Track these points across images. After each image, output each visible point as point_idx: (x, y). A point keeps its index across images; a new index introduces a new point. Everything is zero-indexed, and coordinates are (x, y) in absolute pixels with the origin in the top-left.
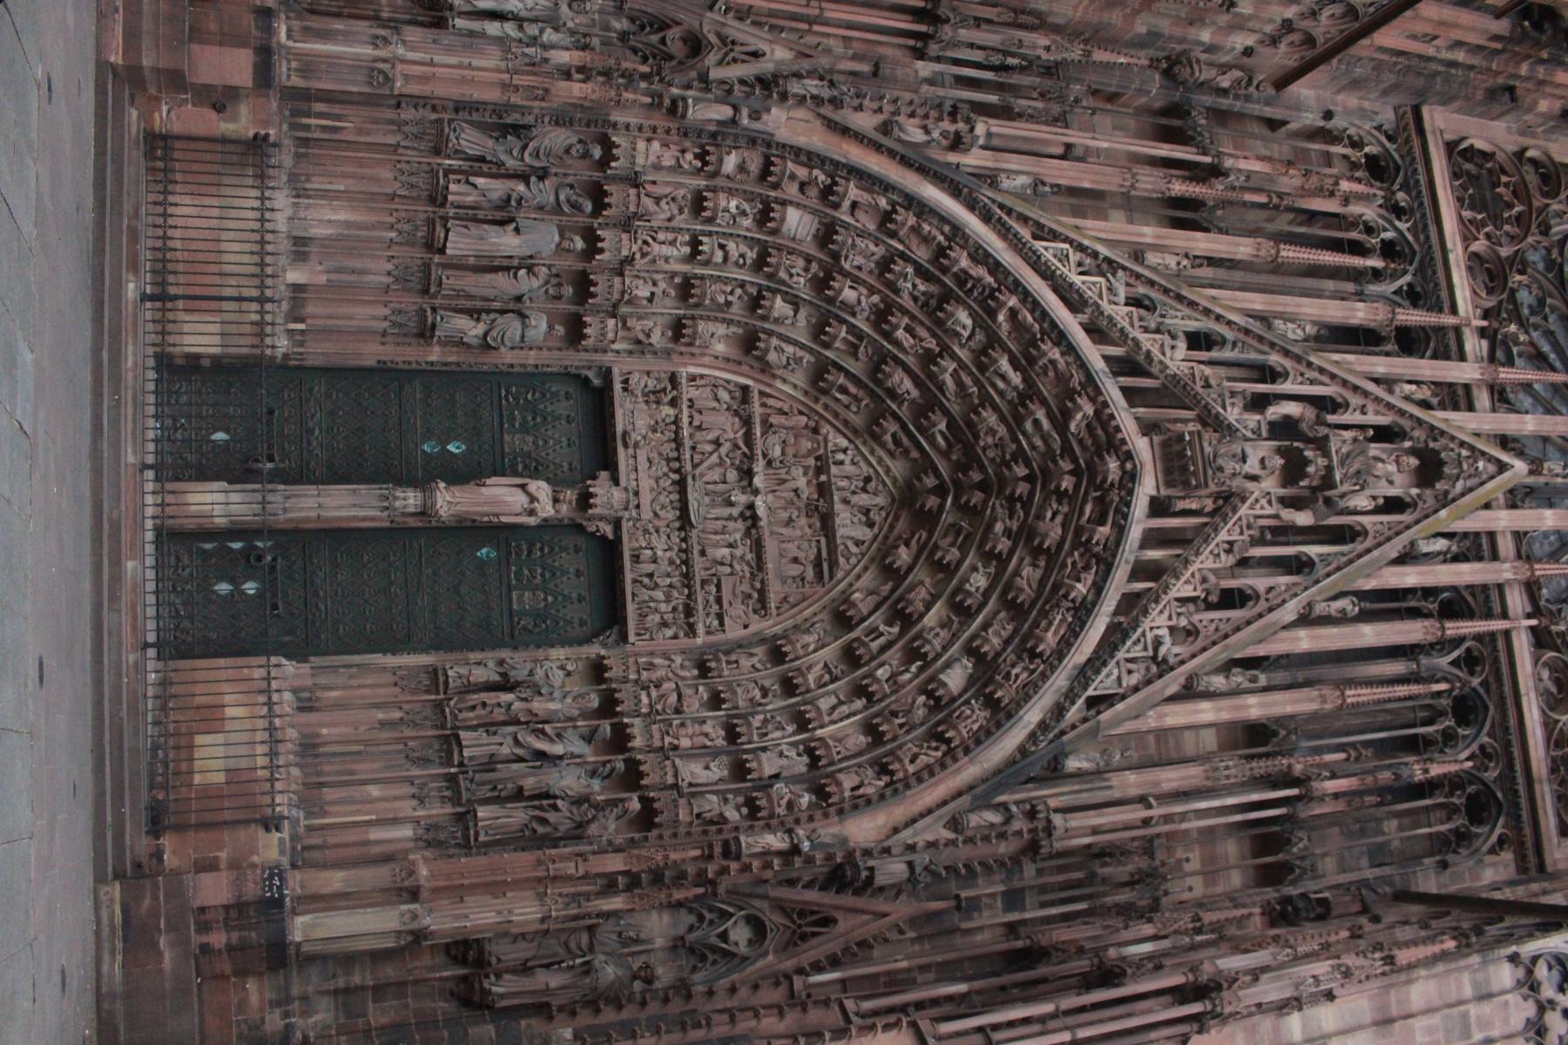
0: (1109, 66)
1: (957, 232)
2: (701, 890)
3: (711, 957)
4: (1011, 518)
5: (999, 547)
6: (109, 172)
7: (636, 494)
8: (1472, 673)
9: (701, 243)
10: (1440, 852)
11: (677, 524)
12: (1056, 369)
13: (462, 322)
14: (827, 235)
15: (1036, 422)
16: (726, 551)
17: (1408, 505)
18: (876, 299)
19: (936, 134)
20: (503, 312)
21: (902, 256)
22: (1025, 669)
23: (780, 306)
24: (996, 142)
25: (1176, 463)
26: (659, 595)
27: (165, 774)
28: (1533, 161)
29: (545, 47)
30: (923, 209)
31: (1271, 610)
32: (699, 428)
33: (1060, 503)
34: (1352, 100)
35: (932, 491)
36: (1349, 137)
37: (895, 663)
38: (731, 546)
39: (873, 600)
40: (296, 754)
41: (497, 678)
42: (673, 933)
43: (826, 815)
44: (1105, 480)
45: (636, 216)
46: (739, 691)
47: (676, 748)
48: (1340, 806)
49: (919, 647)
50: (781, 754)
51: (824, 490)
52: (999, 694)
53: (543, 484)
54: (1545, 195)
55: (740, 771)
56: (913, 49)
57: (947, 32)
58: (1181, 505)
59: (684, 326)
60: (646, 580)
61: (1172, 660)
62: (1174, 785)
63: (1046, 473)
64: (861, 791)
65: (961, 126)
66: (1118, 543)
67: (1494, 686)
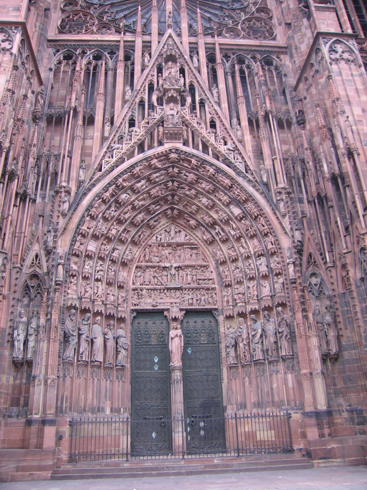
0: (38, 139)
1: (98, 196)
2: (305, 291)
3: (321, 289)
4: (184, 189)
5: (194, 193)
6: (90, 474)
7: (171, 303)
8: (230, 57)
9: (97, 278)
10: (281, 76)
11: (181, 291)
12: (142, 169)
13: (120, 357)
14: (95, 237)
15: (156, 177)
16: (189, 277)
17: (182, 67)
18: (115, 223)
19: (66, 199)
20: (117, 343)
21: (103, 214)
22: (236, 190)
23: (115, 254)
24: (66, 180)
25: (174, 136)
26: (203, 298)
27: (273, 448)
28: (64, 7)
29: (38, 327)
30: (90, 206)
31: (217, 114)
32: (150, 282)
33: (182, 173)
34: (45, 61)
35: (172, 212)
36: (57, 64)
37: (229, 228)
38: (187, 275)
39: (206, 233)
40: (262, 409)
41: (233, 348)
42: (314, 299)
43: (281, 253)
44: (177, 159)
45: (91, 299)
46: (237, 276)
47: (257, 296)
48: (272, 102)
49: (225, 221)
50: (260, 265)
51: (169, 245)
52: (244, 198)
53: (171, 333)
54: (76, 5)
55: (265, 277)
56: (32, 203)
57: (29, 191)
58: (185, 137)
59: (120, 285)
60: (198, 302)
61: (234, 146)
62: (269, 150)
63: (171, 177)
64: (273, 242)
65: (63, 190)
66: (198, 157)
67: (234, 51)
